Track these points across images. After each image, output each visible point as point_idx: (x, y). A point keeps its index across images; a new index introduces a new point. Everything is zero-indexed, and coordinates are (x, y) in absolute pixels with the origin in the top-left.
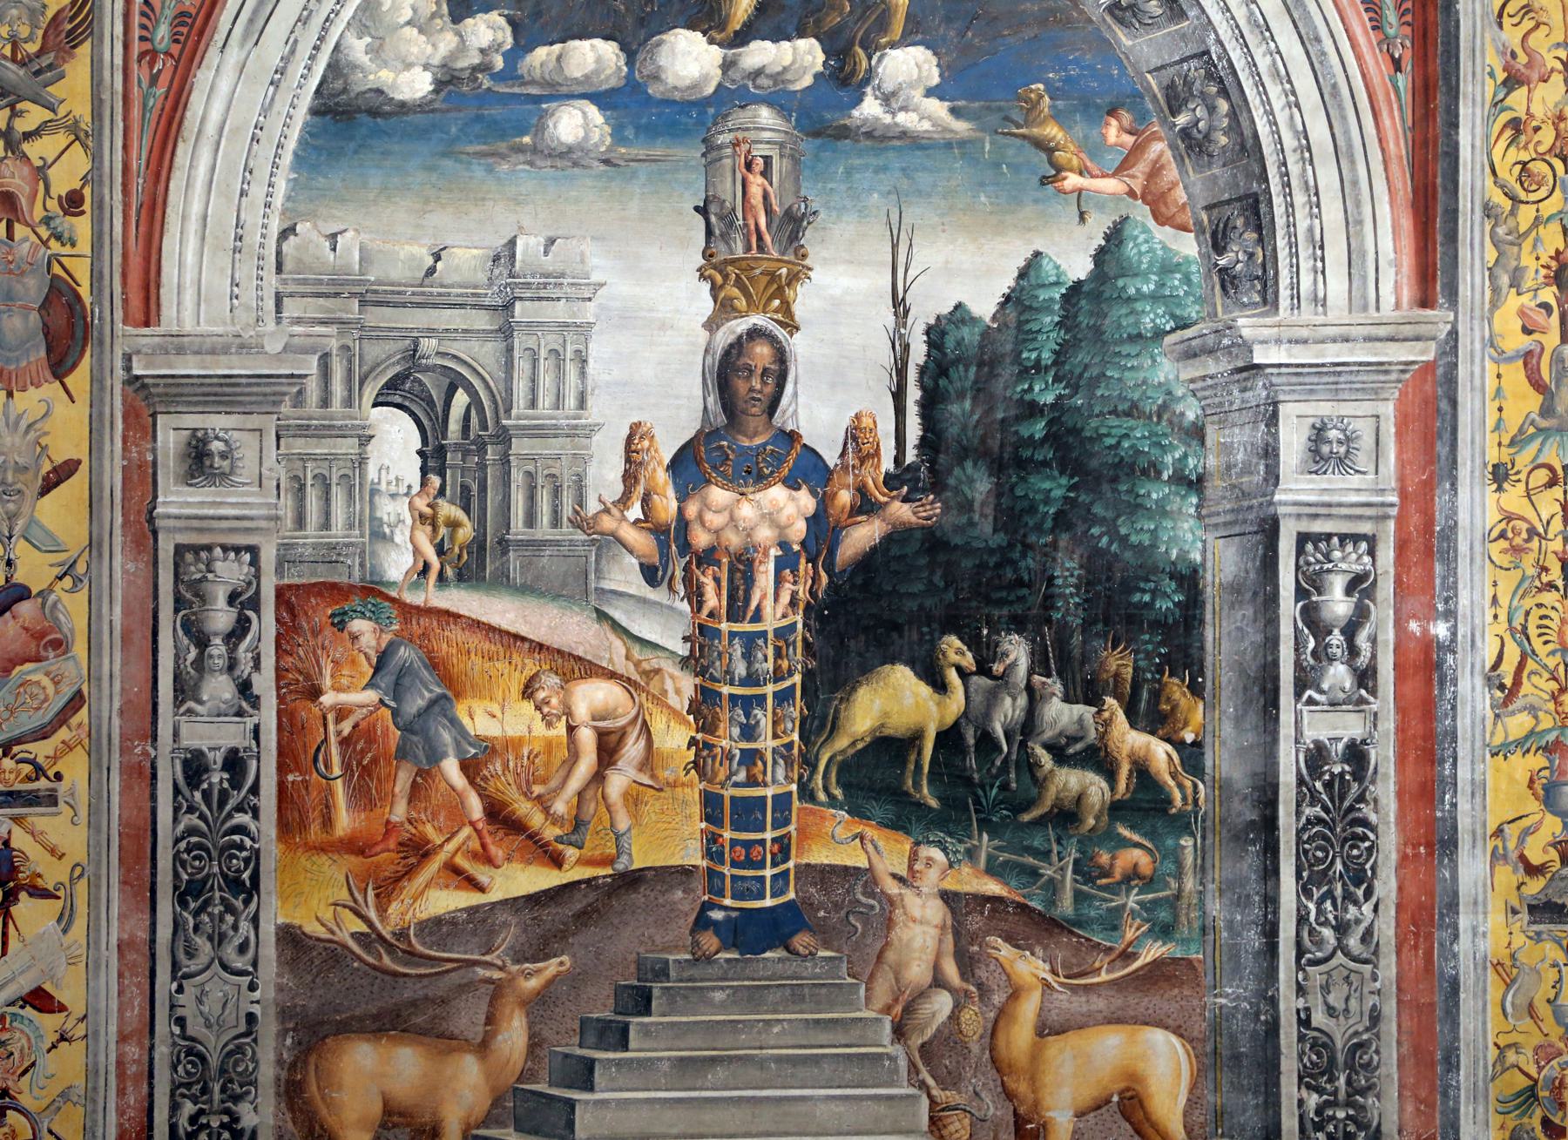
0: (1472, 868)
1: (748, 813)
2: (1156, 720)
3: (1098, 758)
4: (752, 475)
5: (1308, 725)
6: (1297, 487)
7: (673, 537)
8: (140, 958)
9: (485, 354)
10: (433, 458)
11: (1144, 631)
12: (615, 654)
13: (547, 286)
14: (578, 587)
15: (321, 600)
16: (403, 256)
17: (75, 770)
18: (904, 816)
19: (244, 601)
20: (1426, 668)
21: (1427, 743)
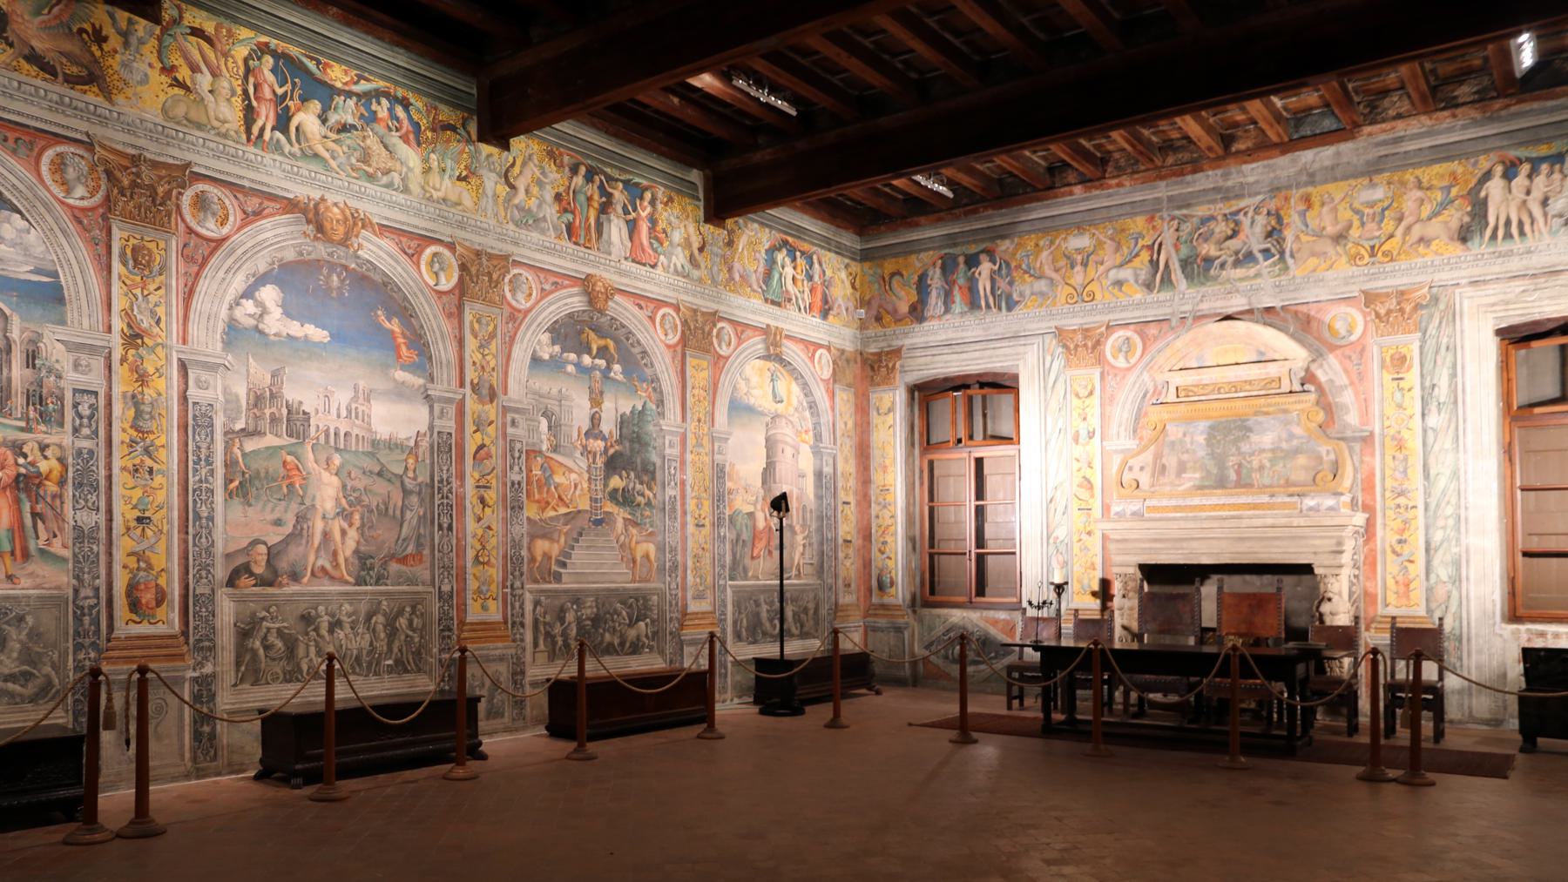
0: (689, 518)
1: (596, 501)
2: (650, 489)
3: (643, 495)
4: (596, 438)
5: (670, 492)
6: (668, 451)
7: (585, 447)
8: (505, 520)
9: (557, 409)
10: (550, 428)
11: (648, 473)
12: (575, 468)
13: (567, 398)
14: (570, 455)
15: (533, 453)
16: (545, 389)
17: (494, 482)
18: (618, 503)
19: (520, 452)
20: (683, 483)
21: (683, 496)
